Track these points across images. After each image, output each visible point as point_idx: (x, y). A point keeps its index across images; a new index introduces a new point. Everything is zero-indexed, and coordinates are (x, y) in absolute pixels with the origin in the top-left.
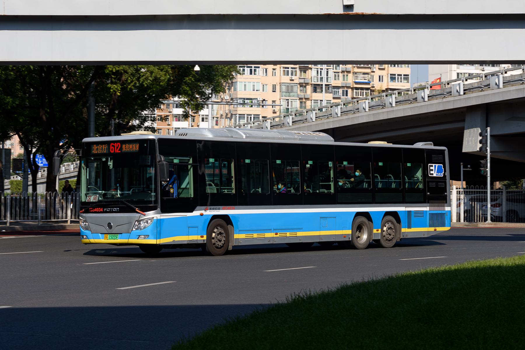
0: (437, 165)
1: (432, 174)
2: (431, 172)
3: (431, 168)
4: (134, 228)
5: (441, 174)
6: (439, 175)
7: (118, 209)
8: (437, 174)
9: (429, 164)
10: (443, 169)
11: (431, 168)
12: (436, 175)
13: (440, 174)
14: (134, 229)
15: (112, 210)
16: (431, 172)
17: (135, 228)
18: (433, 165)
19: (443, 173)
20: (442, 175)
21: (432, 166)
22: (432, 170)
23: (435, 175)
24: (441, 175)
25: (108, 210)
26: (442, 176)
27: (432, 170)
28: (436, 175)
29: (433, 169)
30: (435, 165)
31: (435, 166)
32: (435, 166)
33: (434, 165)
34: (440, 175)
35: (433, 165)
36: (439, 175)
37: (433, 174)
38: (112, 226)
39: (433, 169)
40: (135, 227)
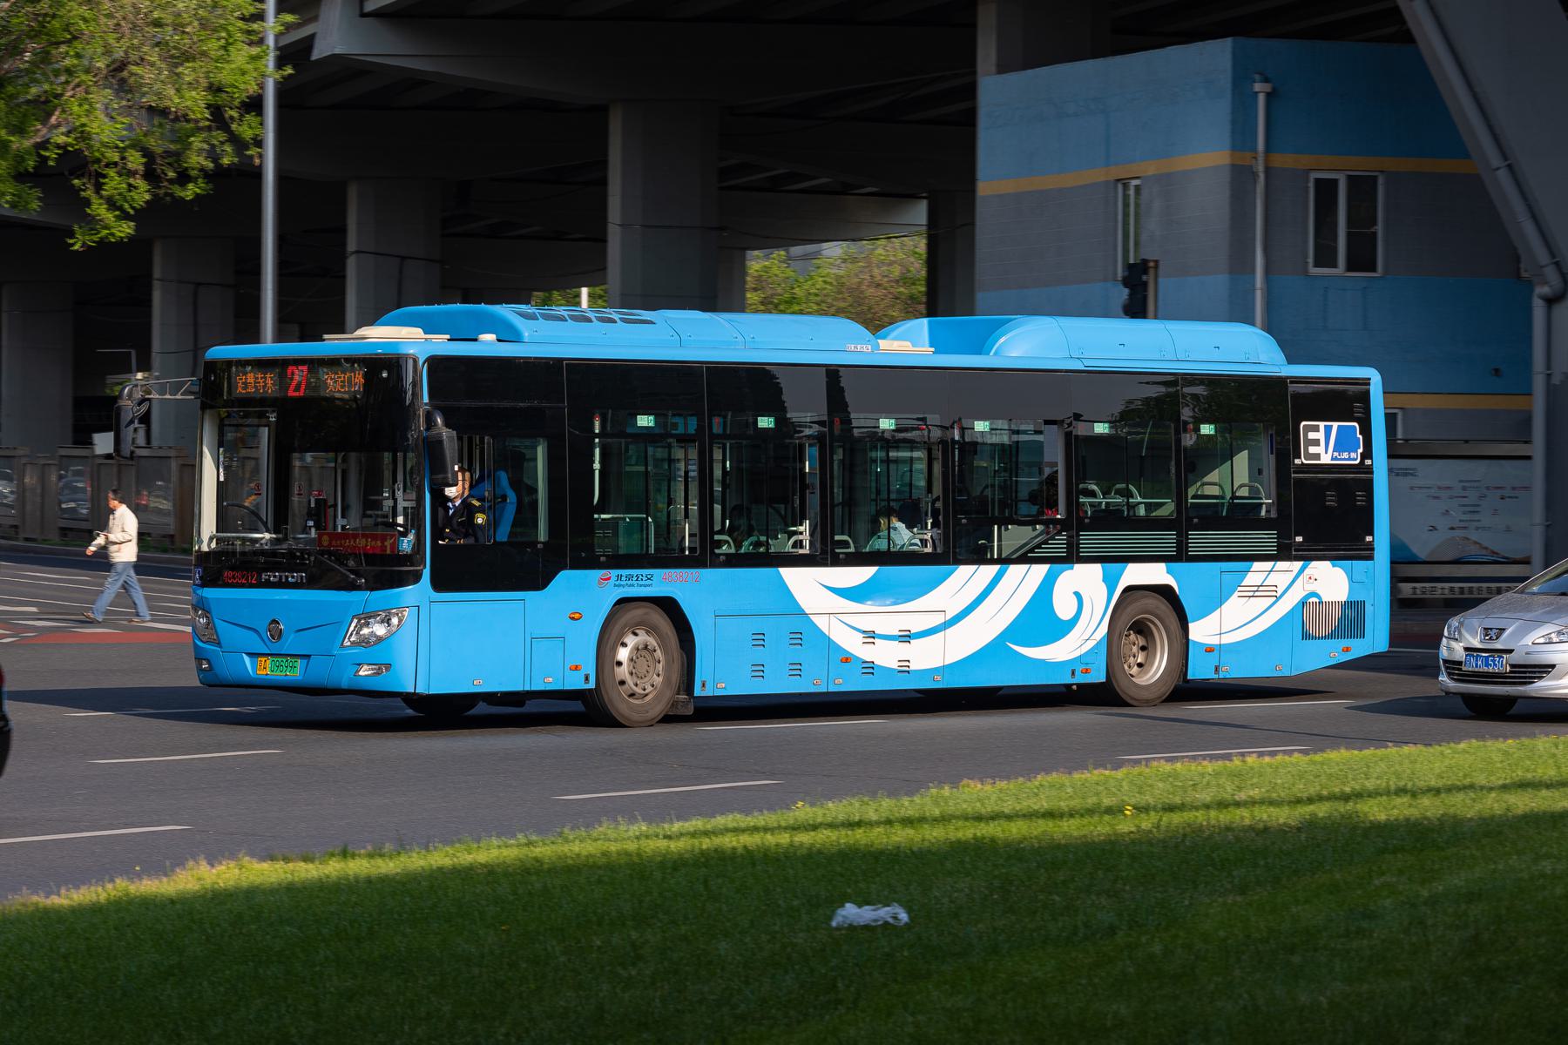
0: (1335, 425)
1: (1317, 456)
2: (1312, 450)
3: (1312, 435)
5: (1353, 455)
7: (302, 577)
9: (1303, 423)
10: (1361, 437)
11: (1312, 435)
12: (1332, 460)
15: (287, 577)
16: (1312, 450)
19: (1360, 450)
20: (1356, 460)
21: (1316, 429)
22: (1316, 443)
23: (1326, 459)
24: (1354, 458)
25: (275, 576)
26: (1357, 462)
27: (1316, 443)
28: (1332, 460)
31: (1328, 430)
32: (1328, 430)
33: (1322, 425)
34: (1349, 459)
37: (1319, 454)
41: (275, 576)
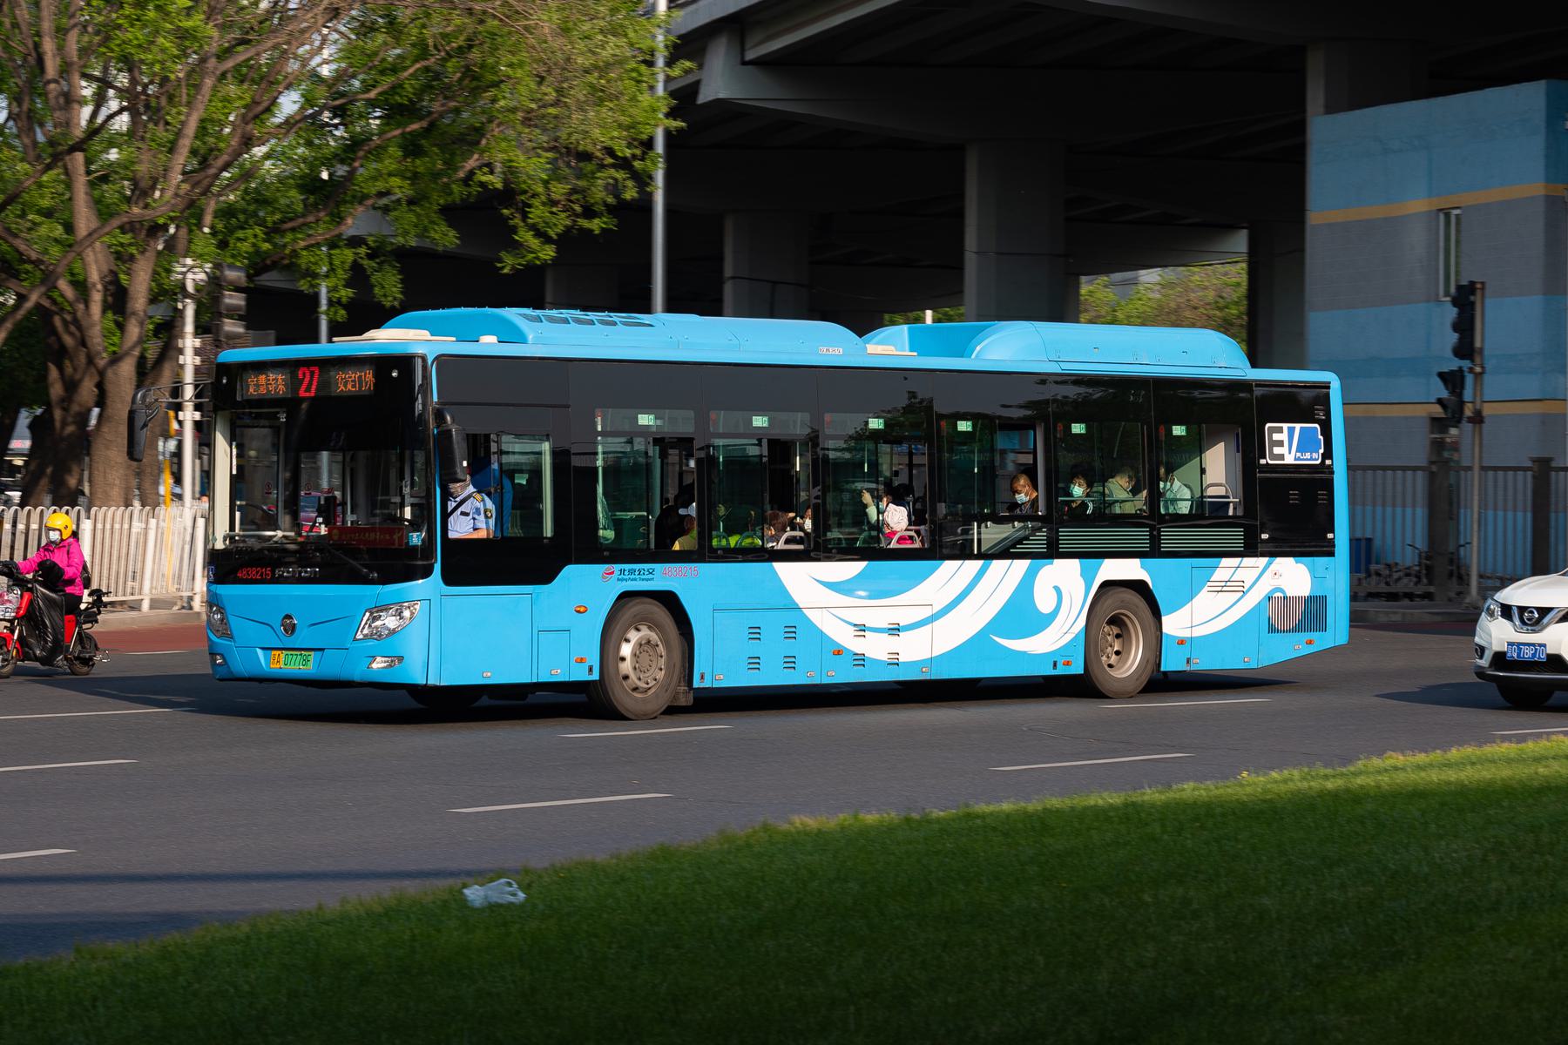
0: (1298, 426)
1: (1281, 457)
2: (1277, 450)
3: (1276, 437)
4: (359, 633)
5: (1315, 455)
6: (1307, 460)
8: (1299, 455)
9: (1268, 425)
10: (1321, 438)
11: (1276, 437)
12: (1295, 459)
13: (1308, 455)
14: (360, 636)
15: (300, 573)
16: (1277, 450)
17: (362, 632)
18: (1282, 427)
19: (1322, 451)
20: (1317, 460)
21: (1280, 430)
22: (1280, 443)
23: (1289, 460)
24: (1313, 458)
26: (1318, 462)
27: (1280, 443)
28: (1295, 459)
29: (1283, 441)
30: (1288, 427)
31: (1291, 431)
32: (1291, 431)
33: (1285, 426)
34: (1311, 459)
35: (1282, 427)
36: (1307, 460)
38: (294, 624)
39: (1283, 441)
40: (364, 628)
41: (288, 572)
